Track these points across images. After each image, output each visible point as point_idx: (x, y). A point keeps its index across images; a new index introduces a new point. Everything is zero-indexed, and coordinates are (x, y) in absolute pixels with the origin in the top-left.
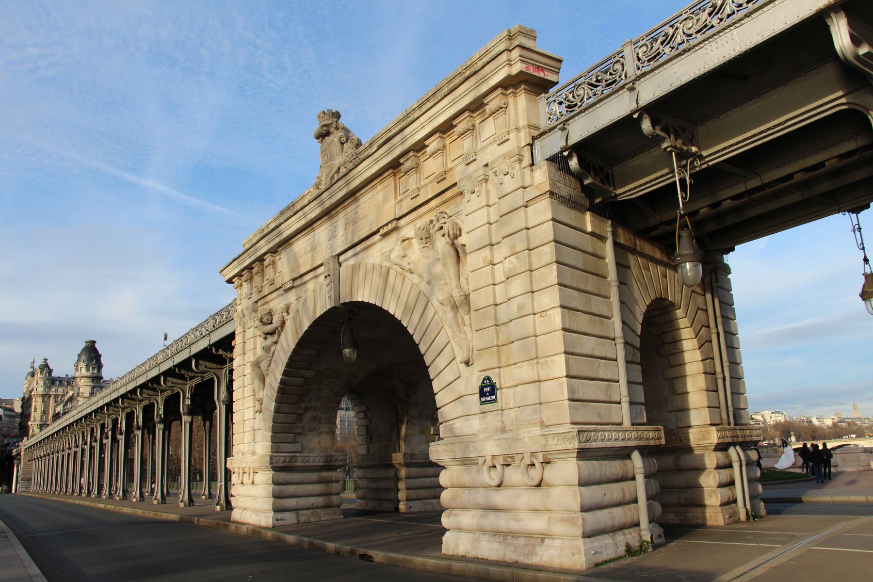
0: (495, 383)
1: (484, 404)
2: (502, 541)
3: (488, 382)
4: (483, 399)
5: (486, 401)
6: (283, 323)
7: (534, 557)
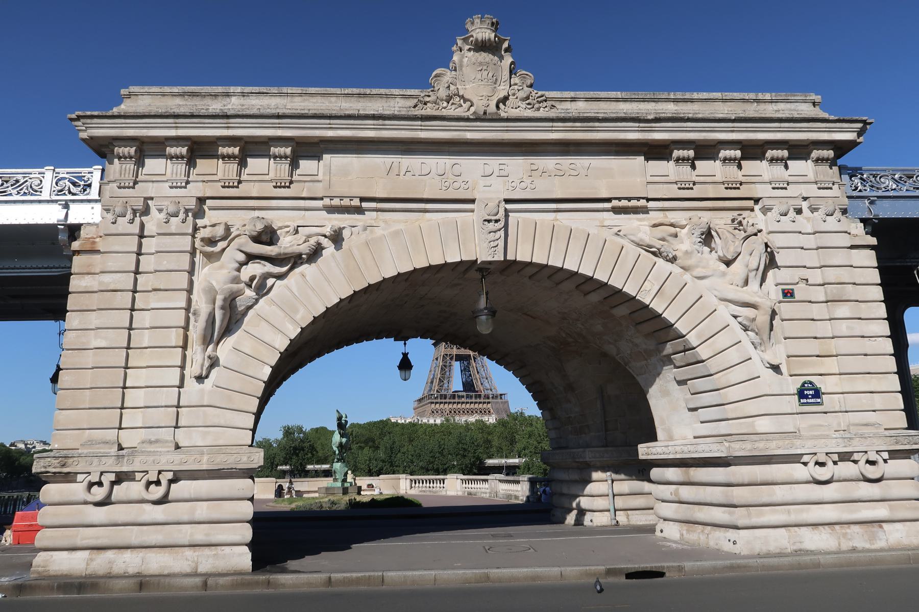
0: (820, 388)
1: (802, 405)
2: (831, 532)
3: (809, 385)
4: (802, 401)
5: (807, 403)
6: (315, 253)
7: (878, 541)
